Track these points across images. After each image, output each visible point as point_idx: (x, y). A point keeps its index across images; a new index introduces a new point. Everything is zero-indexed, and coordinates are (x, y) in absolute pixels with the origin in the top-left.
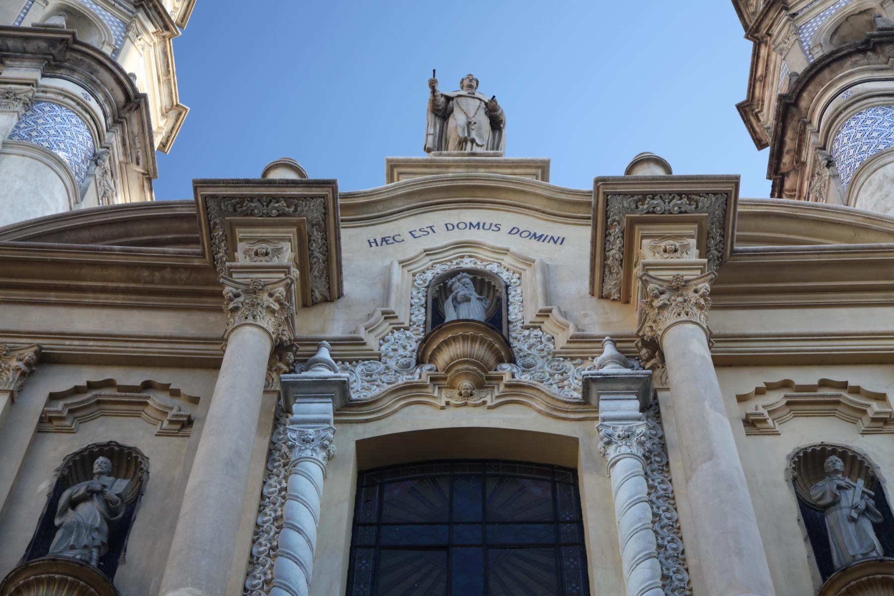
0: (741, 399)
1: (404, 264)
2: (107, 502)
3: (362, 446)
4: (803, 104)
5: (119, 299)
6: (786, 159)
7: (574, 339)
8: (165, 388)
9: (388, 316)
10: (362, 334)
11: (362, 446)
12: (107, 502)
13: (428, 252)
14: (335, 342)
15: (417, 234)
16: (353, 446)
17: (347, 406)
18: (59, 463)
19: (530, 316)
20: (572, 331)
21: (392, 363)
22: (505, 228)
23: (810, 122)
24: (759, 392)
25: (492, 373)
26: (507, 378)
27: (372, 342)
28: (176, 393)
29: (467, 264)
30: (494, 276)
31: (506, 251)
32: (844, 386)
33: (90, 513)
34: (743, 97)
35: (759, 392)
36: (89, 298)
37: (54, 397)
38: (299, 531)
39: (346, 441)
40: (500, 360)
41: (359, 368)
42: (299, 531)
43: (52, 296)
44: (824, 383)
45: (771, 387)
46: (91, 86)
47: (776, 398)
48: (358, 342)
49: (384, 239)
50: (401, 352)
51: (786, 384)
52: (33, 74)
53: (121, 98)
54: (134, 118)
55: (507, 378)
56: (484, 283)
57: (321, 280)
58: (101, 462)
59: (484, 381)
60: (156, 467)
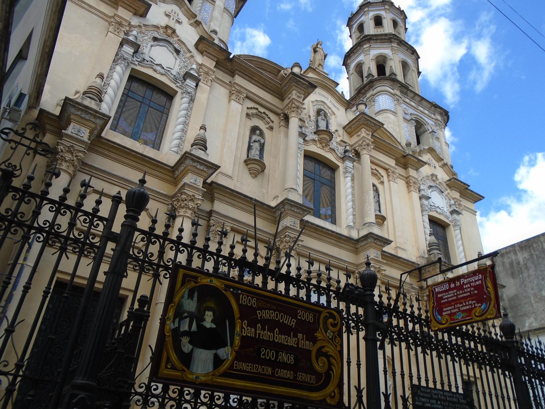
5: (259, 85)
6: (363, 91)
7: (342, 141)
20: (341, 138)
30: (327, 114)
33: (256, 146)
36: (254, 82)
43: (247, 77)
44: (375, 169)
59: (327, 145)
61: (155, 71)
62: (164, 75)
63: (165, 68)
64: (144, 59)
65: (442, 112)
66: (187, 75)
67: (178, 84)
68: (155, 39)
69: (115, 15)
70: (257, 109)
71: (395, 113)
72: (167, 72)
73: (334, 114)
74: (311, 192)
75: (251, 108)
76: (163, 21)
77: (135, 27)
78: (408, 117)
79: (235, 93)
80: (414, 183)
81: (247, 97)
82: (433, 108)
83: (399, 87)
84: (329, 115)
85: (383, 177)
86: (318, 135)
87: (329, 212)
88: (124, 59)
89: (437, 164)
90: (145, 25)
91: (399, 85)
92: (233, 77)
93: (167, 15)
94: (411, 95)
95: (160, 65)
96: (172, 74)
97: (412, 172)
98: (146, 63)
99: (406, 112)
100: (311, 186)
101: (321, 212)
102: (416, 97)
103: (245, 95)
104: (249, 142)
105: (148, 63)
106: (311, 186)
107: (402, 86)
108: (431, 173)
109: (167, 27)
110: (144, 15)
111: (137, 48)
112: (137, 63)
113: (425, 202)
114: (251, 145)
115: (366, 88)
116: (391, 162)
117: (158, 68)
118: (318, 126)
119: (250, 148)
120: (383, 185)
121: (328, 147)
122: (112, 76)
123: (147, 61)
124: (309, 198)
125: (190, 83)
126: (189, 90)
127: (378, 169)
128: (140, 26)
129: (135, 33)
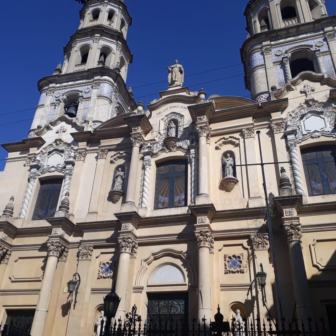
0: (216, 143)
1: (162, 120)
3: (155, 162)
4: (245, 50)
6: (244, 59)
7: (189, 134)
9: (159, 133)
10: (155, 138)
12: (121, 176)
13: (166, 116)
14: (151, 140)
15: (165, 110)
18: (114, 170)
21: (160, 144)
22: (180, 107)
23: (247, 53)
24: (219, 141)
26: (178, 145)
27: (157, 139)
29: (173, 117)
31: (179, 114)
34: (246, 26)
35: (219, 141)
38: (146, 181)
39: (153, 161)
44: (230, 137)
45: (221, 139)
47: (221, 142)
48: (154, 140)
49: (159, 113)
50: (162, 141)
51: (224, 138)
52: (99, 77)
53: (115, 75)
56: (176, 122)
57: (148, 129)
58: (120, 169)
61: (49, 172)
64: (44, 169)
65: (330, 20)
66: (67, 163)
67: (63, 171)
68: (50, 153)
69: (29, 155)
72: (57, 169)
74: (167, 189)
75: (115, 155)
76: (57, 136)
78: (280, 59)
80: (277, 124)
82: (316, 25)
85: (238, 139)
87: (183, 197)
89: (317, 85)
90: (44, 149)
91: (264, 36)
93: (57, 132)
95: (53, 167)
97: (275, 116)
98: (45, 170)
100: (167, 184)
101: (175, 200)
102: (291, 31)
106: (167, 184)
108: (304, 101)
111: (38, 167)
112: (40, 174)
113: (289, 137)
115: (244, 57)
116: (249, 120)
117: (53, 169)
118: (168, 135)
120: (240, 146)
123: (46, 169)
124: (165, 194)
127: (232, 135)
128: (42, 151)
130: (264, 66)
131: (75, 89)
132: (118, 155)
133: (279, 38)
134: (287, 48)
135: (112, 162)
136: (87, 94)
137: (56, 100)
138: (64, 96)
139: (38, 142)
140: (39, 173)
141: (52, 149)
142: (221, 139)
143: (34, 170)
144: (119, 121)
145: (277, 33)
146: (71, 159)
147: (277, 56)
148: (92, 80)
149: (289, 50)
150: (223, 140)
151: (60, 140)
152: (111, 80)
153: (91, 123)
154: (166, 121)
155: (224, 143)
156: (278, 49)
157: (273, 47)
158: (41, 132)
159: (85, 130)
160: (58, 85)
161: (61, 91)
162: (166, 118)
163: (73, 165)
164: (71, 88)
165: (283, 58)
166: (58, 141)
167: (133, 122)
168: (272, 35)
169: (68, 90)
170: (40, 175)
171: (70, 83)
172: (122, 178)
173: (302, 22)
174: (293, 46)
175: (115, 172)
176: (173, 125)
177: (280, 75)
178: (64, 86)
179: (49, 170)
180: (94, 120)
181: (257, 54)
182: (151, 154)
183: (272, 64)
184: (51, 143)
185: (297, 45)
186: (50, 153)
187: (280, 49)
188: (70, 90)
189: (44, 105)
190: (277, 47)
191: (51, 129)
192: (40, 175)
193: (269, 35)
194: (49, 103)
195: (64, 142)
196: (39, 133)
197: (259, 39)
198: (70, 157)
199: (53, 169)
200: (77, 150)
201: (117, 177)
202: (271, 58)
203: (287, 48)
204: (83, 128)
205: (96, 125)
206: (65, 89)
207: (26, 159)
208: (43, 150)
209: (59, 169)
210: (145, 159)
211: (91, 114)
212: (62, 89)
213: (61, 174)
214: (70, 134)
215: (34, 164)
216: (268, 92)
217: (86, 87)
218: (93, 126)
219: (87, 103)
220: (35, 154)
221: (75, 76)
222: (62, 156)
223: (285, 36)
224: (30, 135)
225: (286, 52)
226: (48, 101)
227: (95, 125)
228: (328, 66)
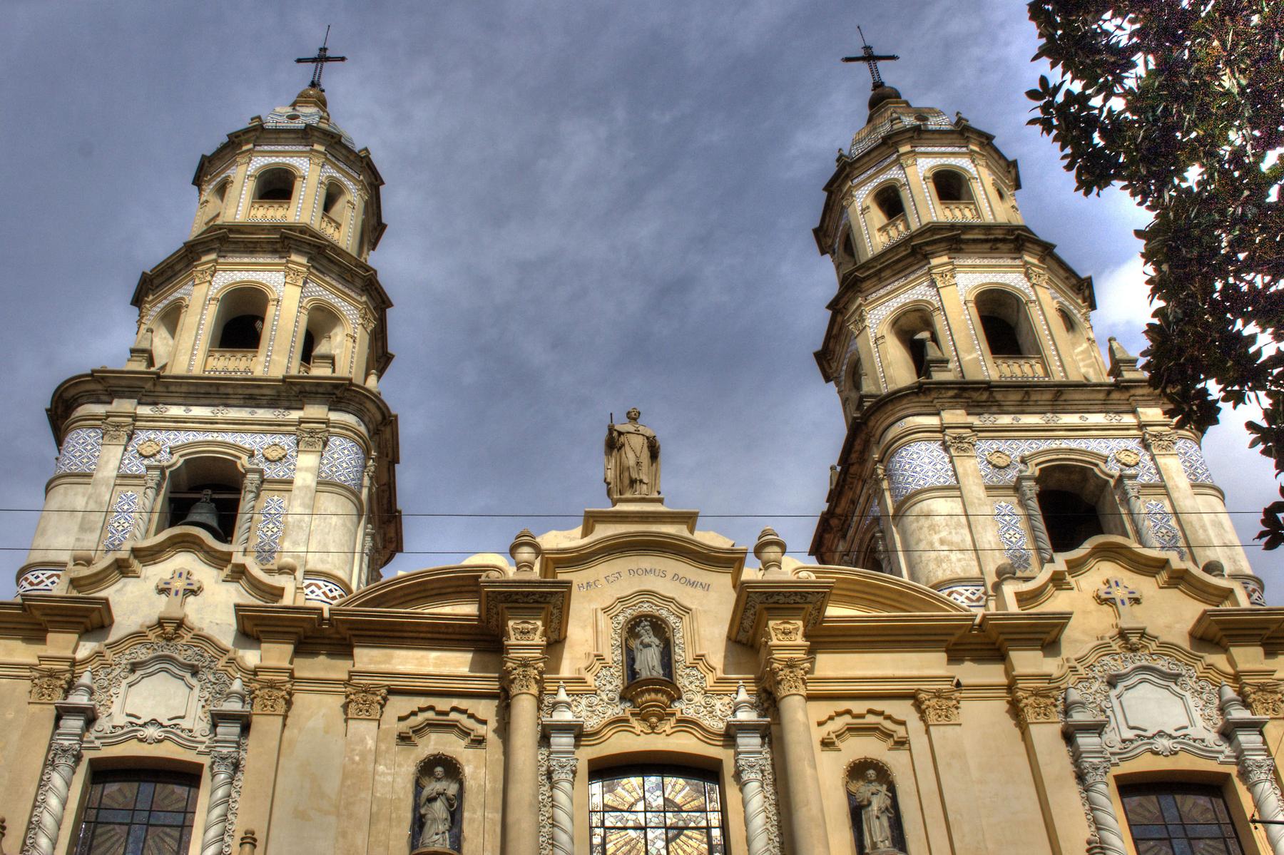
2: (448, 799)
3: (591, 762)
8: (464, 712)
9: (599, 658)
10: (584, 674)
11: (591, 762)
12: (448, 799)
14: (568, 681)
16: (586, 764)
17: (578, 733)
19: (689, 659)
21: (605, 698)
22: (669, 576)
24: (831, 718)
25: (668, 710)
26: (678, 715)
27: (589, 678)
28: (471, 716)
29: (646, 609)
30: (663, 621)
31: (672, 600)
32: (881, 714)
33: (439, 808)
35: (831, 718)
37: (401, 719)
38: (562, 830)
40: (673, 700)
41: (584, 701)
42: (562, 830)
46: (359, 414)
48: (581, 681)
50: (609, 687)
53: (379, 417)
54: (388, 430)
55: (678, 715)
56: (659, 626)
60: (468, 770)
62: (166, 738)
63: (166, 723)
70: (431, 708)
71: (954, 489)
72: (171, 729)
73: (687, 610)
75: (414, 714)
77: (85, 662)
79: (364, 697)
81: (392, 692)
83: (954, 397)
84: (672, 619)
86: (632, 700)
88: (64, 751)
90: (110, 646)
91: (951, 393)
92: (350, 655)
93: (162, 591)
94: (1015, 396)
95: (154, 722)
96: (183, 730)
99: (1002, 463)
103: (384, 691)
104: (416, 807)
105: (126, 730)
107: (965, 389)
109: (161, 623)
110: (107, 622)
112: (97, 743)
114: (423, 811)
117: (152, 732)
119: (419, 823)
121: (673, 720)
122: (44, 801)
125: (229, 731)
126: (225, 751)
128: (99, 654)
129: (86, 679)
130: (958, 493)
131: (219, 439)
132: (430, 715)
133: (994, 409)
134: (1026, 448)
135: (404, 739)
136: (273, 466)
137: (148, 468)
138: (176, 457)
139: (90, 618)
140: (92, 738)
141: (143, 654)
142: (839, 714)
143: (73, 724)
144: (430, 586)
145: (991, 393)
146: (234, 706)
147: (1000, 468)
148: (295, 415)
149: (1033, 456)
150: (847, 719)
151: (180, 624)
152: (363, 429)
153: (299, 574)
154: (621, 618)
155: (852, 729)
156: (995, 446)
157: (980, 434)
158: (100, 579)
159: (287, 600)
160: (145, 411)
161: (162, 436)
162: (619, 607)
163: (246, 729)
164: (206, 431)
165: (1020, 479)
166: (171, 628)
167: (516, 601)
168: (975, 395)
169: (192, 437)
170: (97, 748)
171: (198, 411)
172: (451, 806)
173: (1058, 376)
174: (1044, 445)
175: (418, 787)
176: (649, 638)
177: (1012, 532)
178: (176, 420)
179: (138, 734)
180: (310, 567)
181: (923, 447)
182: (577, 730)
183: (982, 493)
184: (134, 628)
185: (1054, 446)
186: (134, 667)
187: (1002, 445)
188: (201, 437)
189: (90, 476)
190: (993, 438)
191: (134, 572)
192: (97, 748)
193: (966, 395)
194: (115, 473)
195: (196, 632)
196: (82, 582)
197: (929, 399)
198: (229, 696)
199: (152, 732)
200: (255, 671)
201: (431, 800)
202: (972, 469)
203: (1026, 448)
204: (278, 593)
205: (324, 593)
206: (178, 429)
207: (36, 674)
208: (103, 648)
209: (179, 732)
210: (554, 748)
211: (295, 543)
212: (168, 429)
213: (189, 756)
214: (237, 606)
215: (79, 699)
216: (980, 581)
217: (268, 439)
218: (307, 591)
219: (276, 498)
220: (74, 663)
221: (222, 390)
222: (191, 688)
223: (1012, 409)
224: (31, 584)
225: (1023, 461)
226: (107, 462)
227: (313, 588)
228: (1164, 531)
